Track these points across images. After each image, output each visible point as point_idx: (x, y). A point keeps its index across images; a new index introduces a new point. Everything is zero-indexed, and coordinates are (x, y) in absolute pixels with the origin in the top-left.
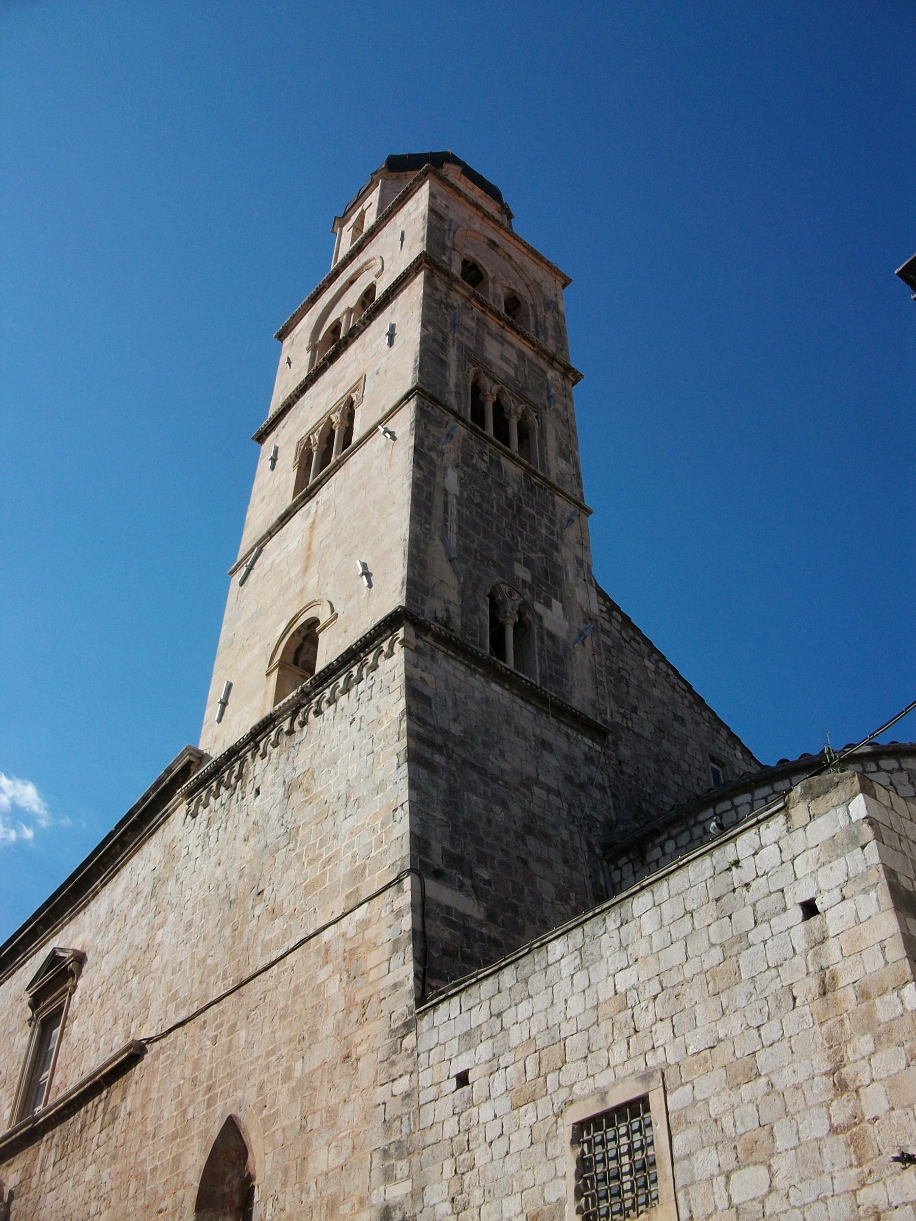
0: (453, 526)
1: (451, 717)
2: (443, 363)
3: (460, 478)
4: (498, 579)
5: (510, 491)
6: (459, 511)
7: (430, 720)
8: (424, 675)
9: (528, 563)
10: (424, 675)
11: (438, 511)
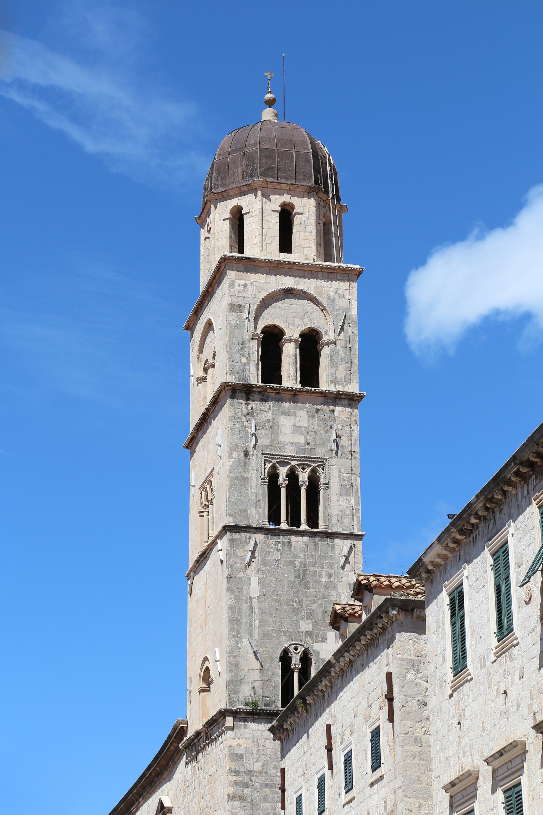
0: (256, 623)
1: (255, 760)
2: (246, 480)
3: (260, 579)
4: (286, 645)
5: (297, 563)
6: (259, 608)
7: (242, 769)
8: (241, 742)
9: (309, 617)
10: (241, 742)
11: (245, 619)
